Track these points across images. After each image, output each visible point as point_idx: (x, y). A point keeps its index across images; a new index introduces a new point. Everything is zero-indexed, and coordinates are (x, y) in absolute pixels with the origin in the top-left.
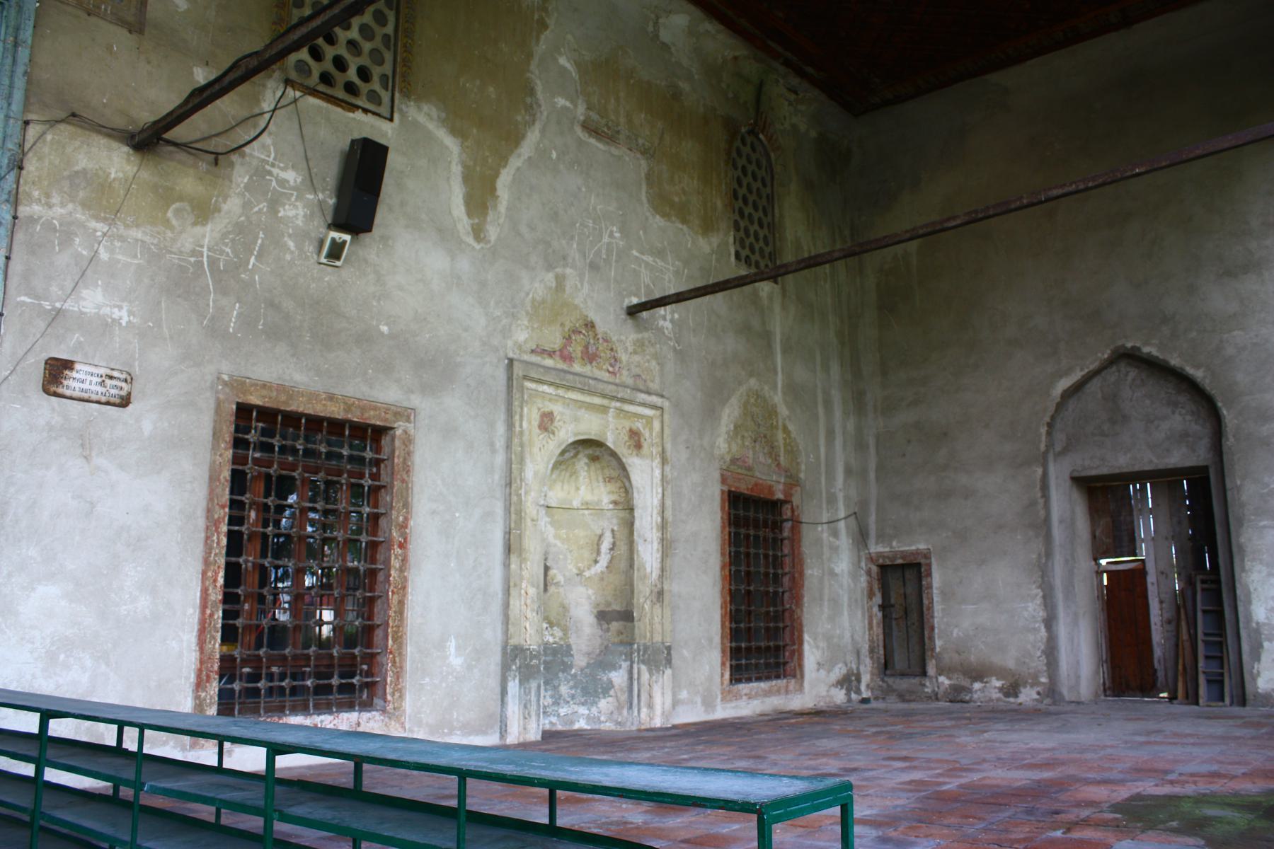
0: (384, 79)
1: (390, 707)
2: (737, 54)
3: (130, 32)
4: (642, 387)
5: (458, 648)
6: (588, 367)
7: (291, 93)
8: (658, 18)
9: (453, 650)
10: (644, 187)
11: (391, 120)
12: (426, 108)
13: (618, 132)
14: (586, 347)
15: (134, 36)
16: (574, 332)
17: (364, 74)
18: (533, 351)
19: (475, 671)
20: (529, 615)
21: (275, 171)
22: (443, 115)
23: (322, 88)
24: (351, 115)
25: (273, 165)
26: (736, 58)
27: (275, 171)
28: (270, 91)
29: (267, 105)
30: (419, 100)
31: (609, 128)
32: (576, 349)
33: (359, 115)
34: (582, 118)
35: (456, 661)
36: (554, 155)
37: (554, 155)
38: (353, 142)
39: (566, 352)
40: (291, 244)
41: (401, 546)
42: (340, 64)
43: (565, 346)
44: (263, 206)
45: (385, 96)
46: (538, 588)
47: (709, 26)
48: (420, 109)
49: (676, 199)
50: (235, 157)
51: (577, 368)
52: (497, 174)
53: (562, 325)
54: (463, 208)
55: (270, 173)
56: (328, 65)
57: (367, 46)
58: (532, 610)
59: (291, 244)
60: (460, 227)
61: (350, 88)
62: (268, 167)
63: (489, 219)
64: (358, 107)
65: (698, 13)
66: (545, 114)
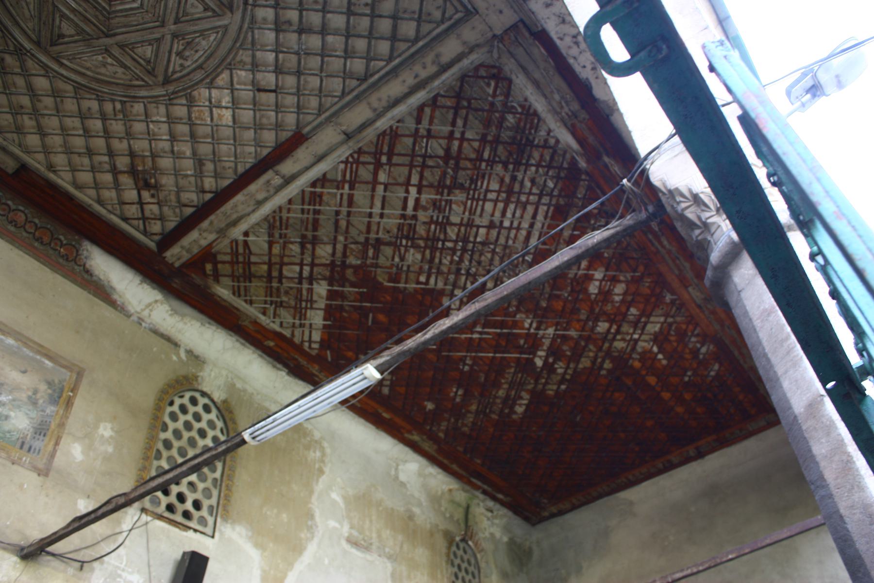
0: (211, 508)
2: (451, 487)
3: (39, 475)
7: (144, 517)
8: (398, 465)
11: (213, 537)
12: (238, 528)
13: (371, 544)
15: (41, 478)
17: (197, 505)
21: (124, 574)
22: (250, 534)
23: (167, 514)
24: (184, 533)
25: (123, 570)
26: (450, 490)
27: (124, 574)
28: (130, 515)
29: (126, 526)
30: (234, 522)
31: (365, 541)
33: (191, 533)
34: (346, 535)
36: (326, 561)
37: (326, 561)
38: (184, 554)
42: (181, 498)
45: (210, 520)
47: (433, 470)
48: (234, 529)
50: (96, 564)
55: (120, 576)
56: (173, 499)
57: (201, 486)
61: (187, 515)
62: (119, 572)
64: (190, 528)
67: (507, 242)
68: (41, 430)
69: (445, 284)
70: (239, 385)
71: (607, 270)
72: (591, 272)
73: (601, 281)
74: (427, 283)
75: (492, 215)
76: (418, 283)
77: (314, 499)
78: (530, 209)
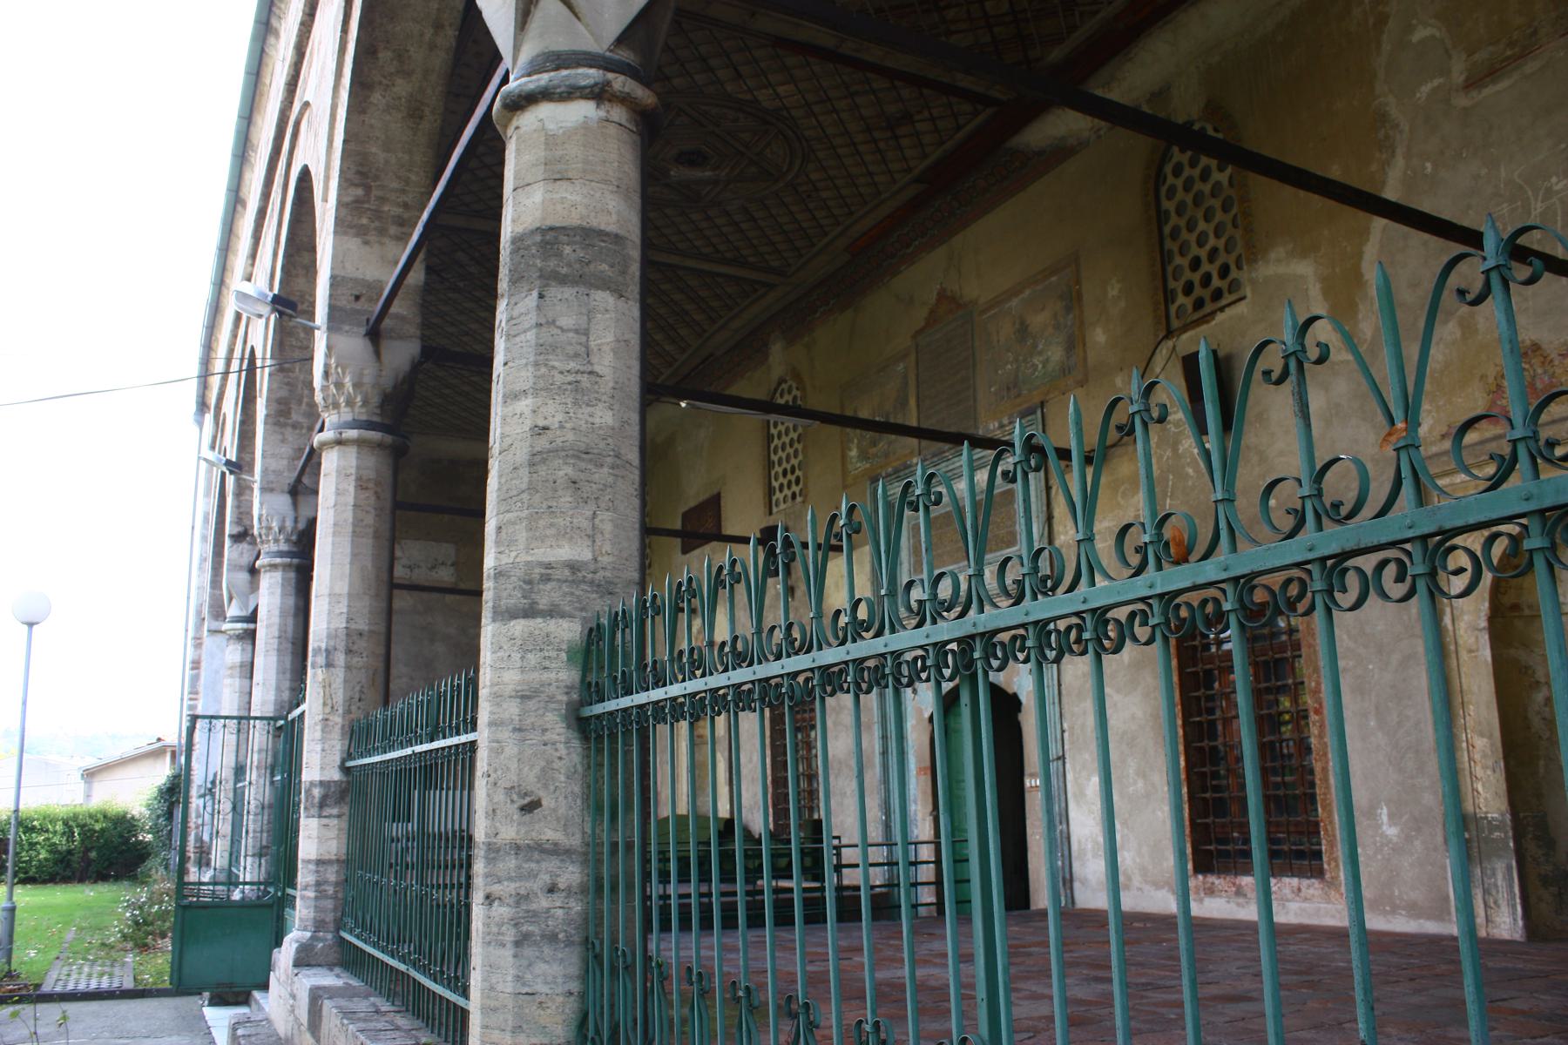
1: (1327, 876)
5: (1390, 816)
7: (1170, 343)
9: (1385, 818)
12: (1273, 255)
19: (1417, 843)
20: (1479, 772)
33: (1220, 317)
35: (1392, 831)
40: (1190, 471)
41: (1317, 712)
43: (1493, 403)
44: (1169, 453)
46: (1491, 737)
52: (1359, 255)
53: (1483, 377)
58: (1485, 768)
59: (1190, 471)
66: (1407, 128)
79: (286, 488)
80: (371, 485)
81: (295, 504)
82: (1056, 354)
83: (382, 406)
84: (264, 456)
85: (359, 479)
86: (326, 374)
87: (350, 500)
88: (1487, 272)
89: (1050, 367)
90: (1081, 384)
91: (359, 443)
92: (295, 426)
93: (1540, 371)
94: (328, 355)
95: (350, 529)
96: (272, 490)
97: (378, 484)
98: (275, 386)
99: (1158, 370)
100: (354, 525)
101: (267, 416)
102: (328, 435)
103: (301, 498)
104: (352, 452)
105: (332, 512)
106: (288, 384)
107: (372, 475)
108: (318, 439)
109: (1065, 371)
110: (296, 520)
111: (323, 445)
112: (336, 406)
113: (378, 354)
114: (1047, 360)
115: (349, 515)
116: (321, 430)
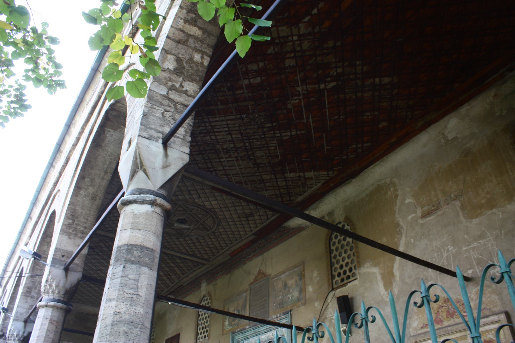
2: (493, 94)
4: (488, 314)
6: (452, 320)
7: (333, 292)
8: (443, 134)
10: (461, 214)
12: (366, 266)
13: (439, 203)
14: (448, 311)
16: (439, 308)
18: (422, 328)
26: (495, 95)
31: (433, 206)
32: (443, 315)
33: (349, 285)
39: (438, 320)
43: (437, 317)
47: (463, 110)
49: (483, 201)
51: (446, 324)
54: (384, 290)
60: (384, 297)
63: (394, 286)
65: (453, 114)
66: (405, 228)
67: (237, 127)
68: (301, 292)
69: (274, 140)
70: (348, 204)
71: (241, 79)
72: (244, 87)
73: (249, 79)
74: (275, 147)
75: (224, 135)
76: (276, 149)
77: (397, 216)
78: (213, 124)
79: (23, 320)
80: (55, 323)
81: (25, 326)
82: (296, 294)
83: (64, 295)
84: (17, 307)
85: (51, 320)
86: (47, 281)
87: (46, 328)
88: (422, 297)
89: (294, 298)
90: (304, 304)
91: (54, 307)
92: (31, 297)
93: (450, 307)
94: (49, 275)
95: (43, 339)
96: (17, 320)
97: (57, 322)
98: (28, 282)
99: (329, 301)
100: (45, 337)
101: (22, 292)
102: (43, 303)
103: (28, 324)
104: (50, 310)
105: (38, 332)
106: (32, 282)
107: (56, 319)
108: (39, 304)
109: (299, 300)
110: (24, 332)
111: (40, 306)
112: (48, 293)
113: (66, 276)
114: (293, 296)
115: (44, 333)
116: (41, 301)
